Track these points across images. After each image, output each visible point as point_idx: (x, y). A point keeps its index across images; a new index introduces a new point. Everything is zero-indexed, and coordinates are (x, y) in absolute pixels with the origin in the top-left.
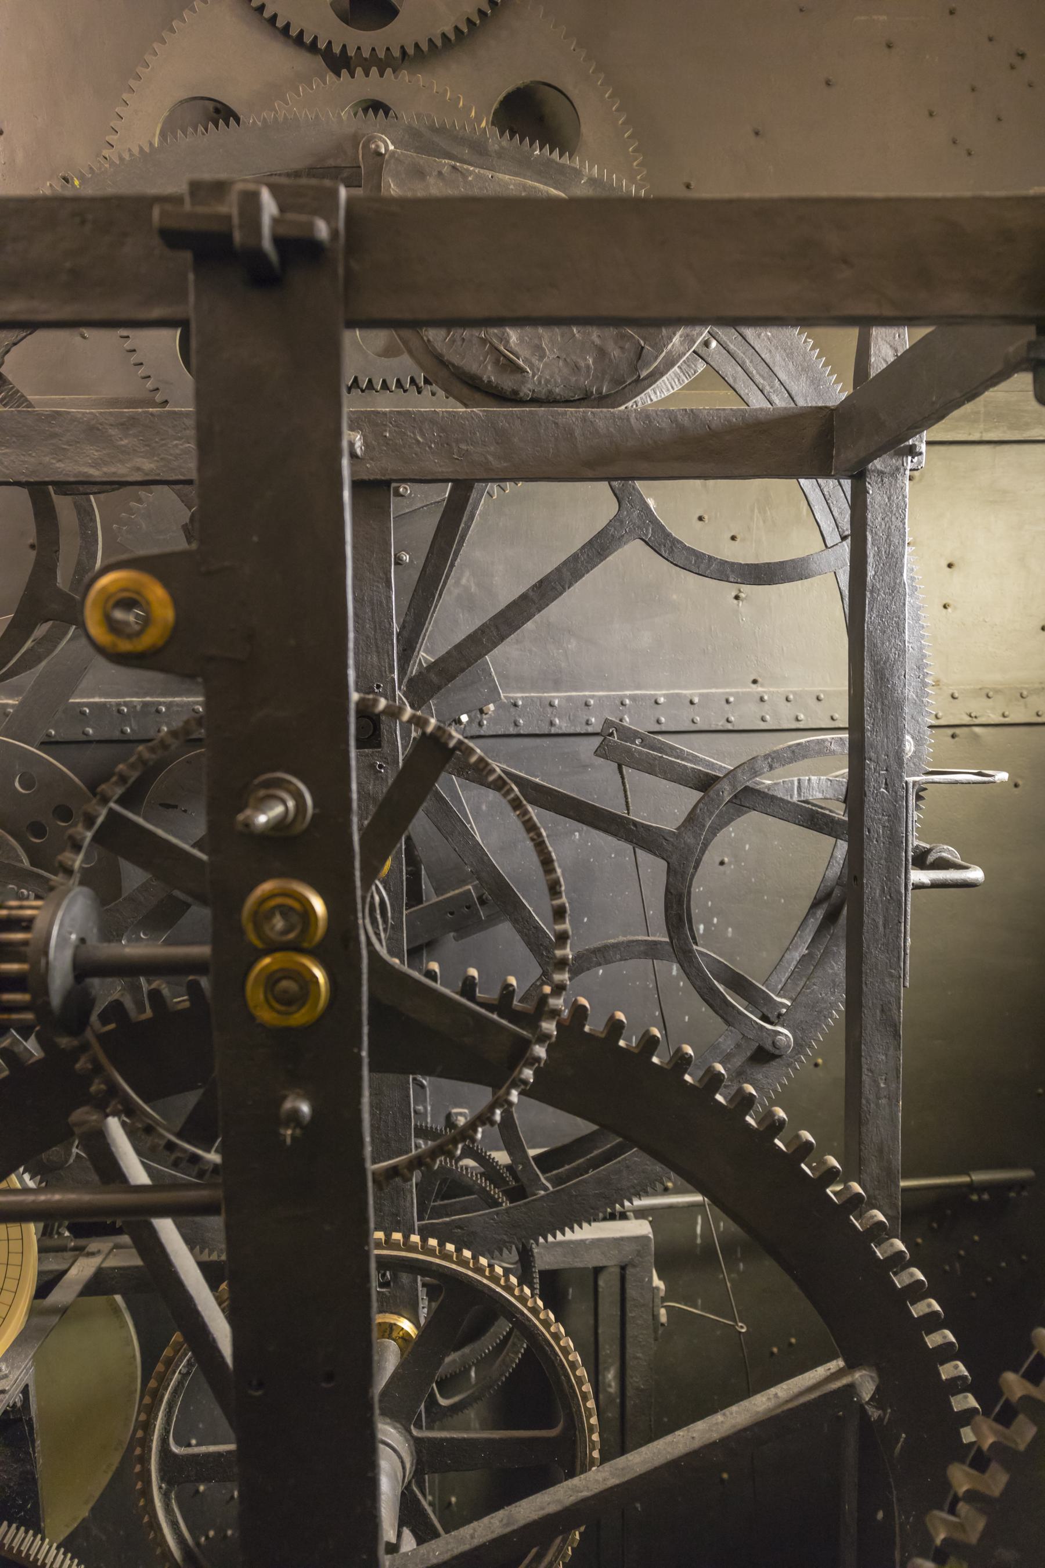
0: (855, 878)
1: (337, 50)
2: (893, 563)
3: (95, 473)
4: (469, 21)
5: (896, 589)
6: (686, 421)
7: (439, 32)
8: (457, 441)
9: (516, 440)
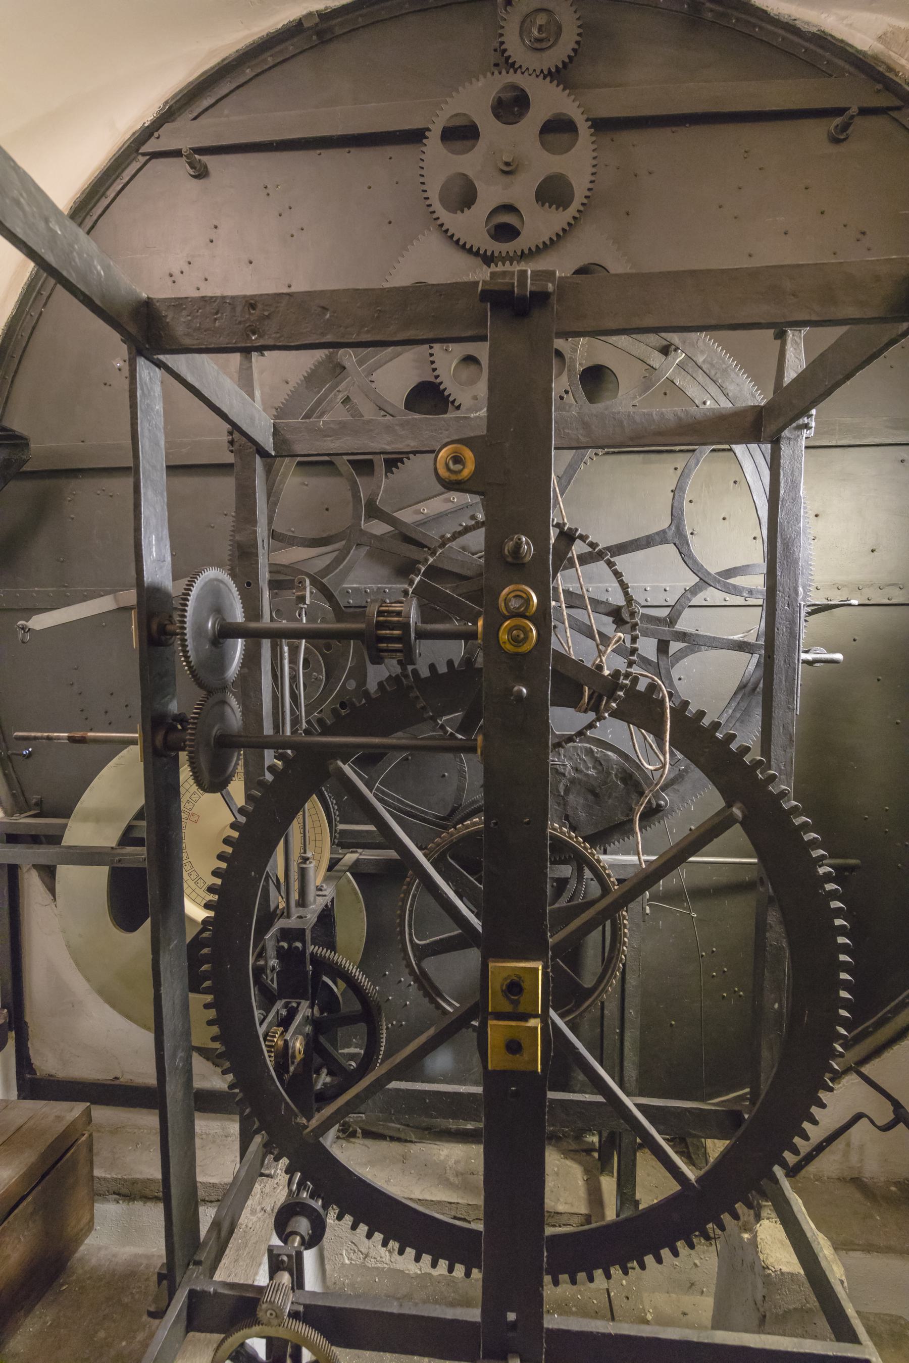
0: (769, 657)
1: (489, 253)
2: (794, 486)
4: (557, 235)
5: (796, 500)
6: (682, 415)
7: (541, 241)
8: (563, 429)
9: (593, 427)
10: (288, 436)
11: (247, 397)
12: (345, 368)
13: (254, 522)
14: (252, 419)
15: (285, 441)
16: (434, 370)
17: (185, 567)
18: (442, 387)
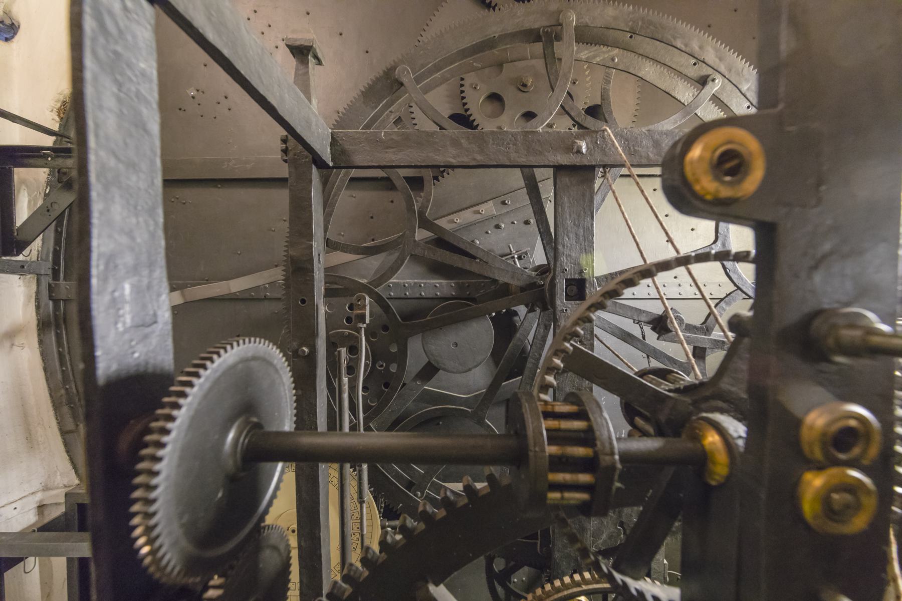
3: (454, 162)
10: (347, 147)
11: (302, 96)
12: (402, 84)
13: (310, 236)
14: (308, 123)
15: (343, 152)
16: (465, 104)
17: (199, 328)
18: (472, 118)
